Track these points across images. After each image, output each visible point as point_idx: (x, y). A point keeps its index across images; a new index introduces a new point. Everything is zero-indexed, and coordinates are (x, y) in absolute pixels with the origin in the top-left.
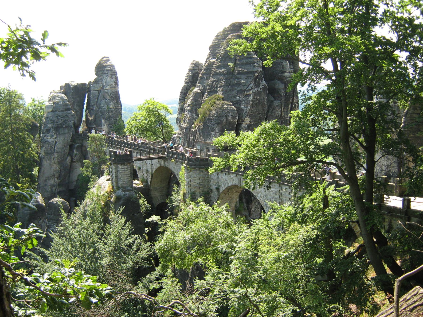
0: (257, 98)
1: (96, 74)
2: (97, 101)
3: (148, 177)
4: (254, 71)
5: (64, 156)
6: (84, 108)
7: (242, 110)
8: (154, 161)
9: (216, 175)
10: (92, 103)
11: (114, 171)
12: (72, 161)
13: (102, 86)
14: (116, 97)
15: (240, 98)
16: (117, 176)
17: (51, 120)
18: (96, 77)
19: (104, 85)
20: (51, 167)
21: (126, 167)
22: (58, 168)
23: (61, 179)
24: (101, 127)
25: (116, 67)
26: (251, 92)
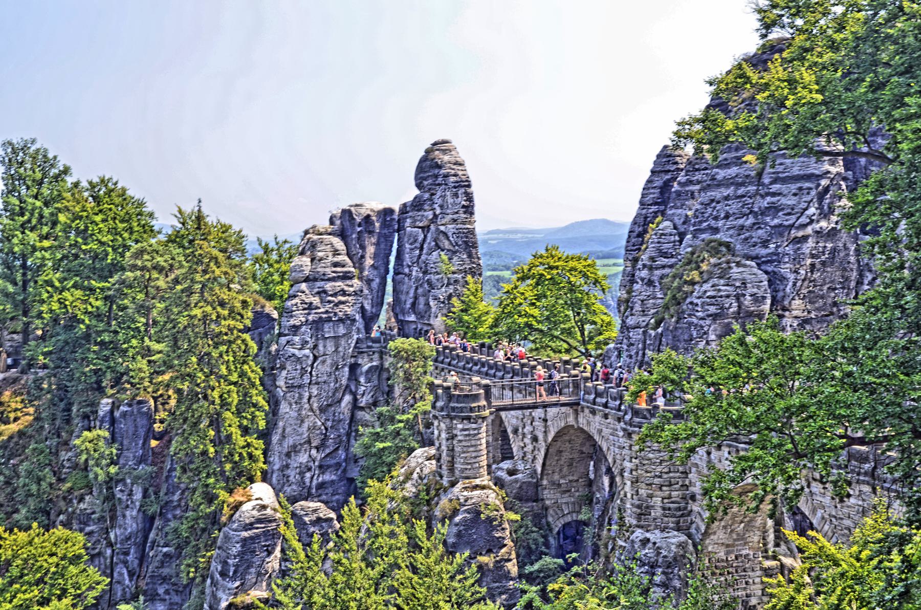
0: (825, 247)
1: (419, 186)
2: (419, 256)
3: (536, 452)
4: (817, 172)
5: (334, 394)
6: (387, 272)
7: (783, 279)
8: (552, 411)
9: (705, 454)
10: (407, 260)
11: (444, 435)
12: (355, 406)
13: (431, 217)
14: (468, 243)
15: (777, 247)
16: (451, 450)
17: (303, 302)
18: (417, 192)
19: (438, 211)
20: (302, 421)
21: (474, 426)
22: (319, 423)
23: (328, 451)
24: (429, 320)
25: (468, 166)
26: (809, 230)
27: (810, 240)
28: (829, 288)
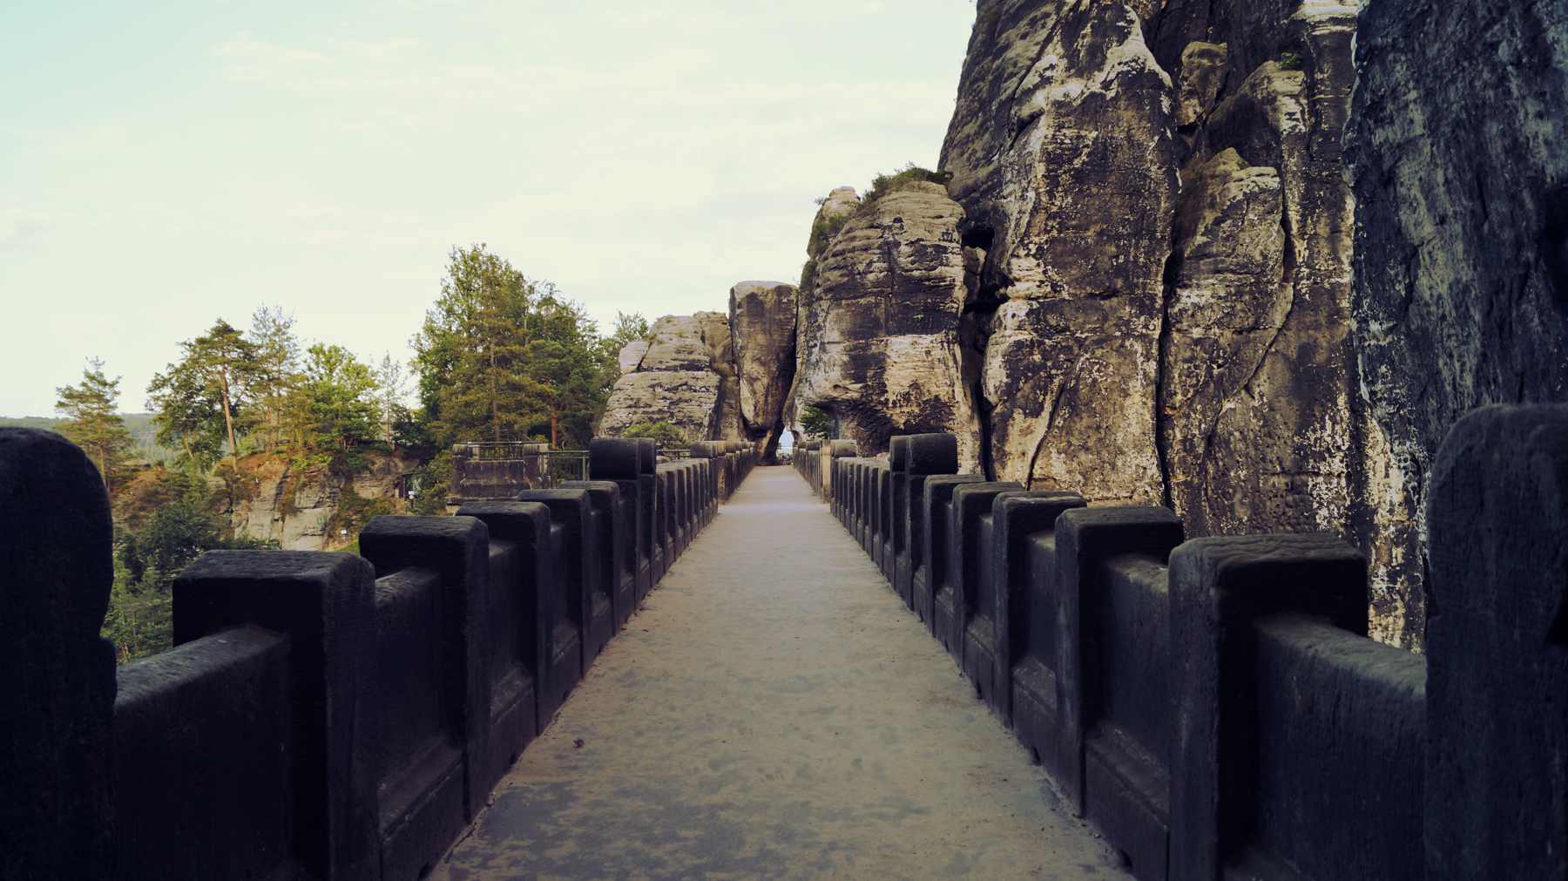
0: (1079, 137)
26: (1040, 100)
27: (1043, 121)
28: (1100, 234)
